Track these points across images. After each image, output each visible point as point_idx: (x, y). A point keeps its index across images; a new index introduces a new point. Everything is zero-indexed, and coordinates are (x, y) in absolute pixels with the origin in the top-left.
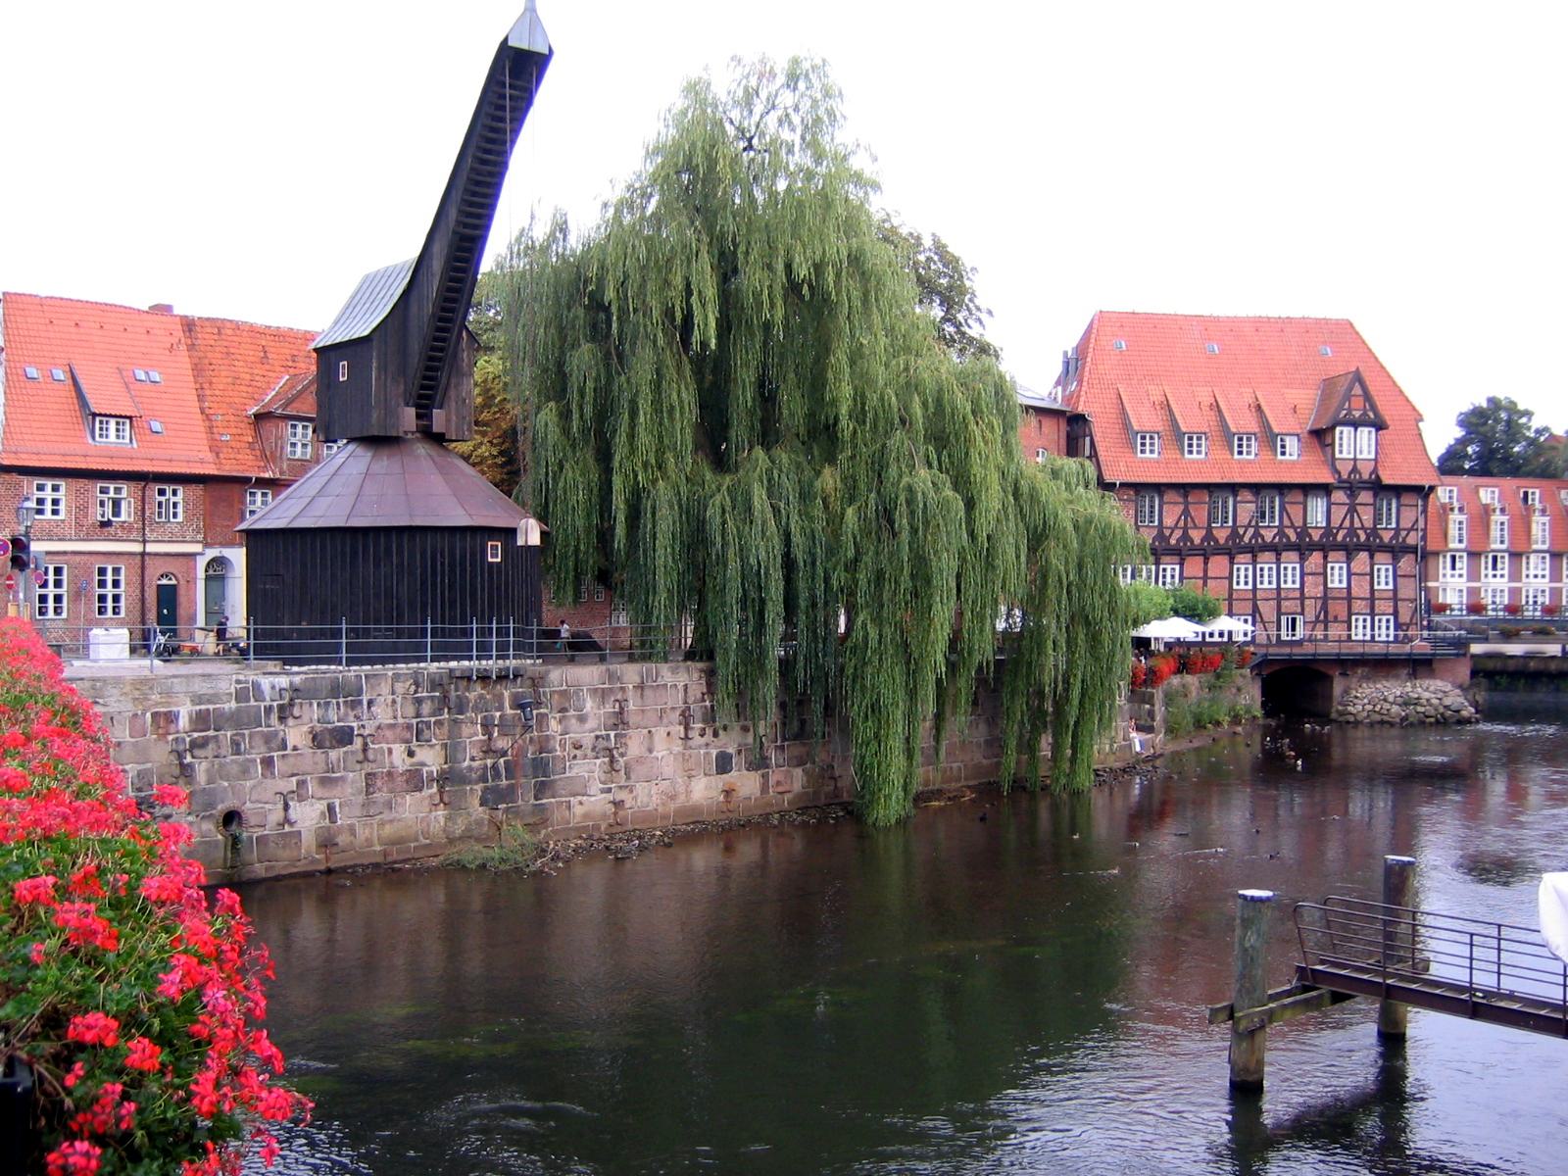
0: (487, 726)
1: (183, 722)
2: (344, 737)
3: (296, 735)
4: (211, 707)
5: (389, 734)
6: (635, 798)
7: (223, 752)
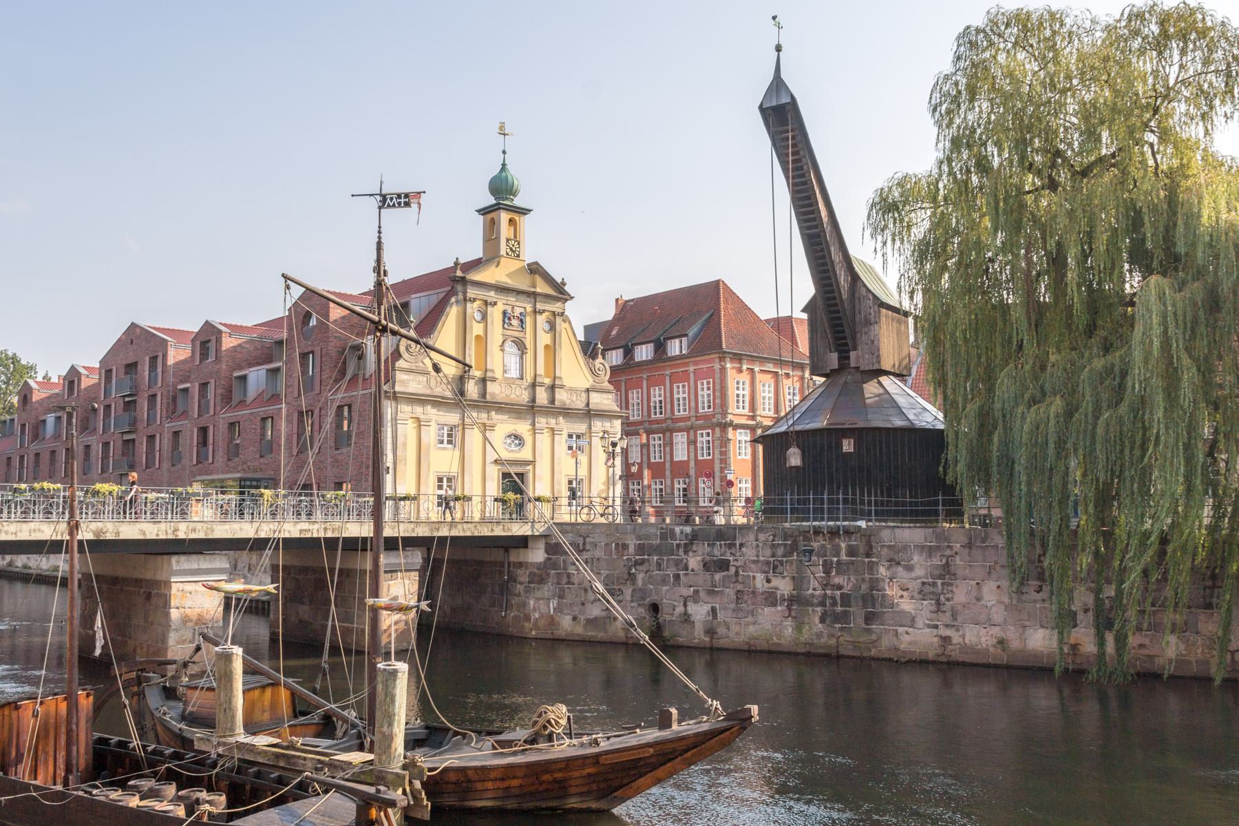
0: (827, 568)
1: (631, 549)
2: (723, 565)
6: (963, 636)
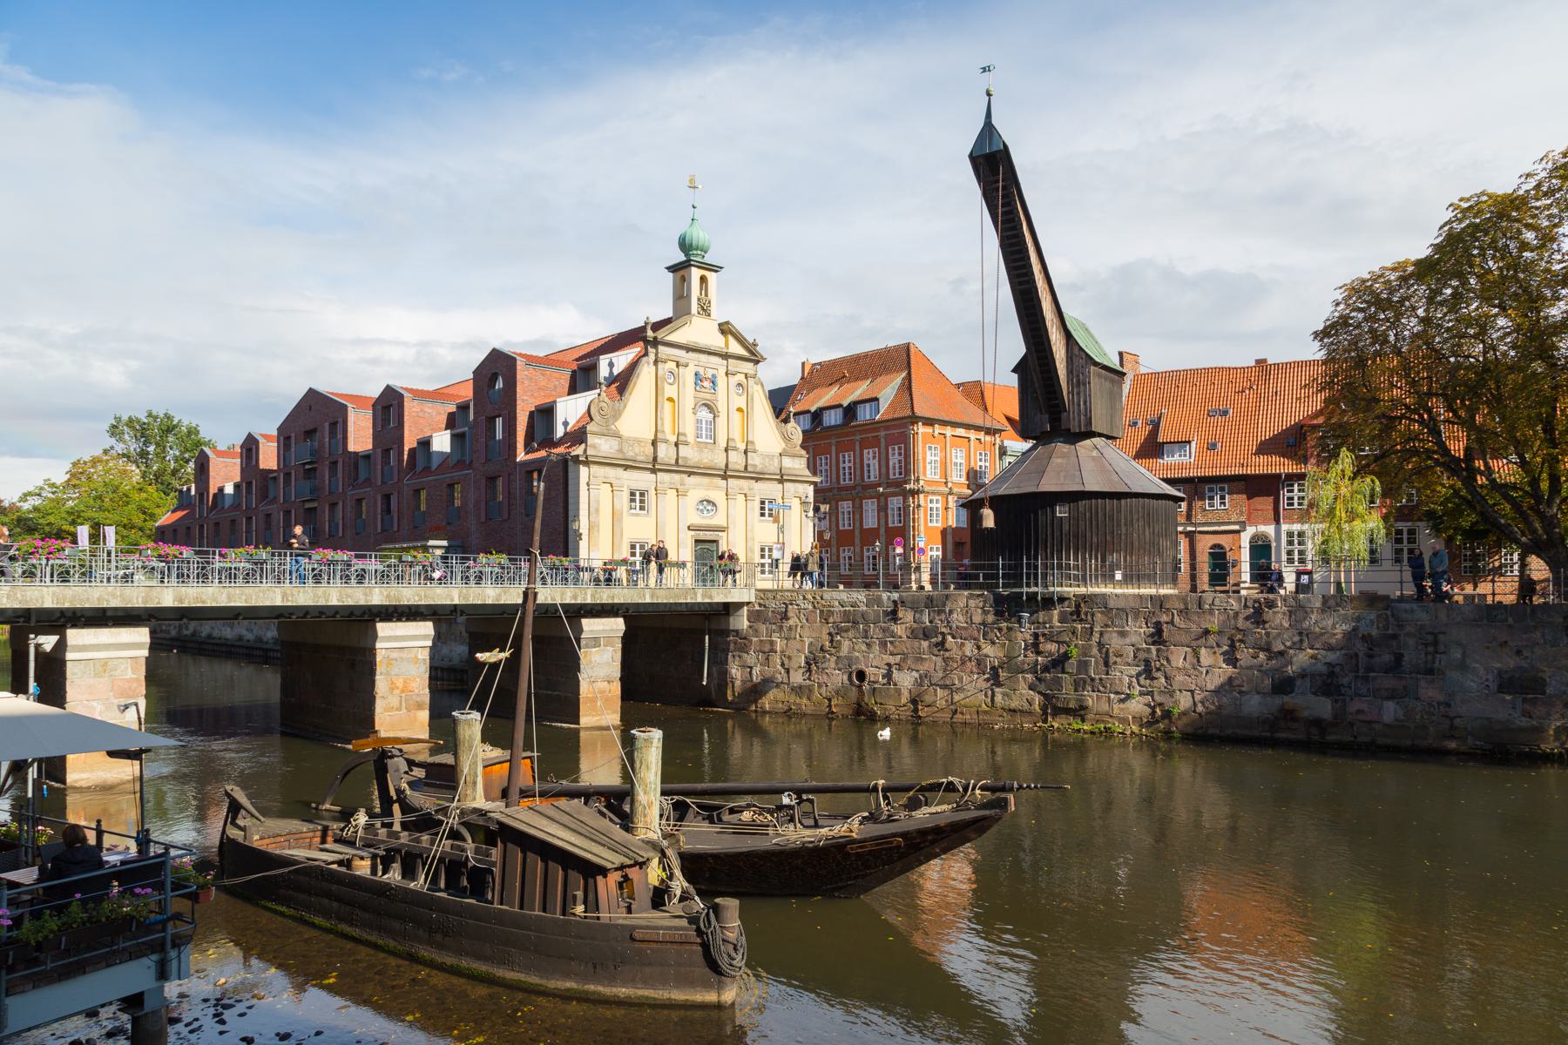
3: (899, 630)
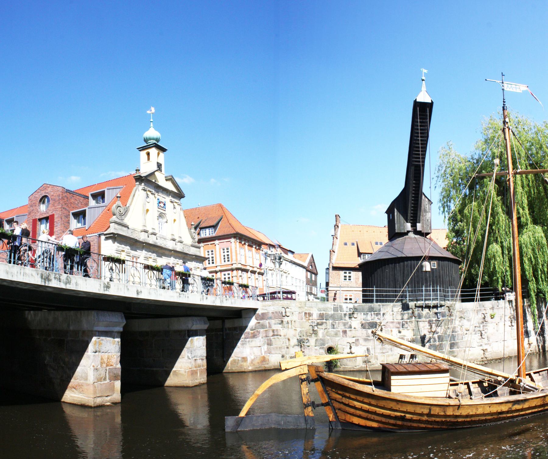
0: (430, 322)
1: (315, 316)
3: (356, 323)
4: (324, 312)
5: (391, 325)
7: (328, 327)
